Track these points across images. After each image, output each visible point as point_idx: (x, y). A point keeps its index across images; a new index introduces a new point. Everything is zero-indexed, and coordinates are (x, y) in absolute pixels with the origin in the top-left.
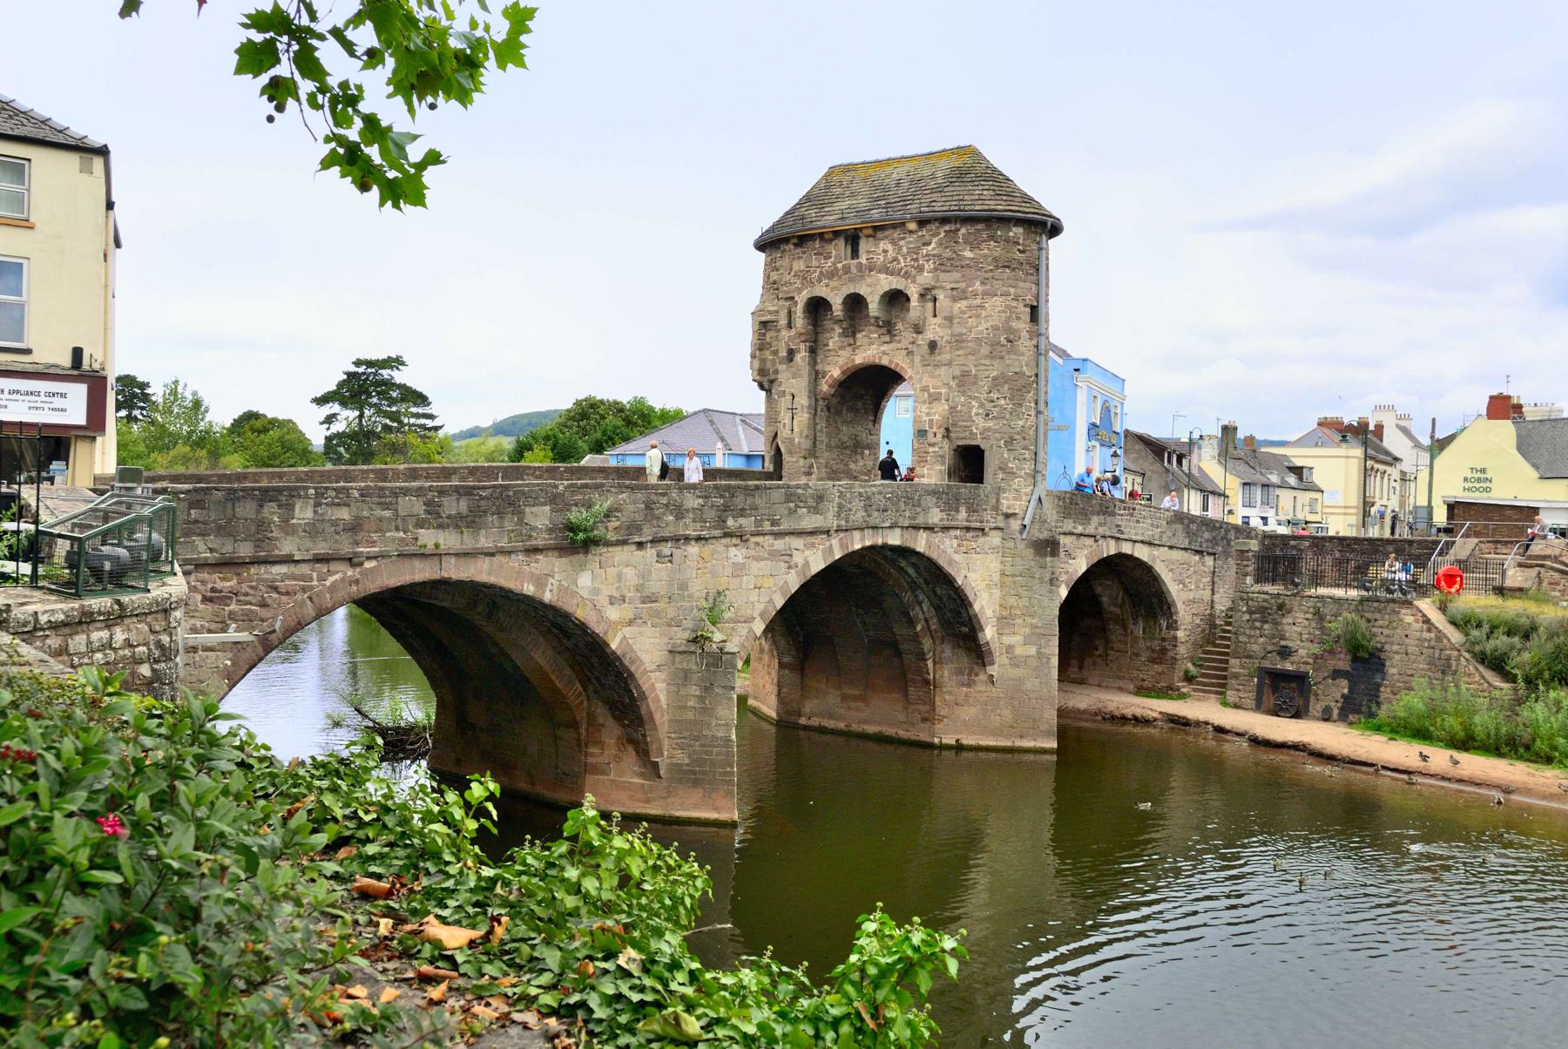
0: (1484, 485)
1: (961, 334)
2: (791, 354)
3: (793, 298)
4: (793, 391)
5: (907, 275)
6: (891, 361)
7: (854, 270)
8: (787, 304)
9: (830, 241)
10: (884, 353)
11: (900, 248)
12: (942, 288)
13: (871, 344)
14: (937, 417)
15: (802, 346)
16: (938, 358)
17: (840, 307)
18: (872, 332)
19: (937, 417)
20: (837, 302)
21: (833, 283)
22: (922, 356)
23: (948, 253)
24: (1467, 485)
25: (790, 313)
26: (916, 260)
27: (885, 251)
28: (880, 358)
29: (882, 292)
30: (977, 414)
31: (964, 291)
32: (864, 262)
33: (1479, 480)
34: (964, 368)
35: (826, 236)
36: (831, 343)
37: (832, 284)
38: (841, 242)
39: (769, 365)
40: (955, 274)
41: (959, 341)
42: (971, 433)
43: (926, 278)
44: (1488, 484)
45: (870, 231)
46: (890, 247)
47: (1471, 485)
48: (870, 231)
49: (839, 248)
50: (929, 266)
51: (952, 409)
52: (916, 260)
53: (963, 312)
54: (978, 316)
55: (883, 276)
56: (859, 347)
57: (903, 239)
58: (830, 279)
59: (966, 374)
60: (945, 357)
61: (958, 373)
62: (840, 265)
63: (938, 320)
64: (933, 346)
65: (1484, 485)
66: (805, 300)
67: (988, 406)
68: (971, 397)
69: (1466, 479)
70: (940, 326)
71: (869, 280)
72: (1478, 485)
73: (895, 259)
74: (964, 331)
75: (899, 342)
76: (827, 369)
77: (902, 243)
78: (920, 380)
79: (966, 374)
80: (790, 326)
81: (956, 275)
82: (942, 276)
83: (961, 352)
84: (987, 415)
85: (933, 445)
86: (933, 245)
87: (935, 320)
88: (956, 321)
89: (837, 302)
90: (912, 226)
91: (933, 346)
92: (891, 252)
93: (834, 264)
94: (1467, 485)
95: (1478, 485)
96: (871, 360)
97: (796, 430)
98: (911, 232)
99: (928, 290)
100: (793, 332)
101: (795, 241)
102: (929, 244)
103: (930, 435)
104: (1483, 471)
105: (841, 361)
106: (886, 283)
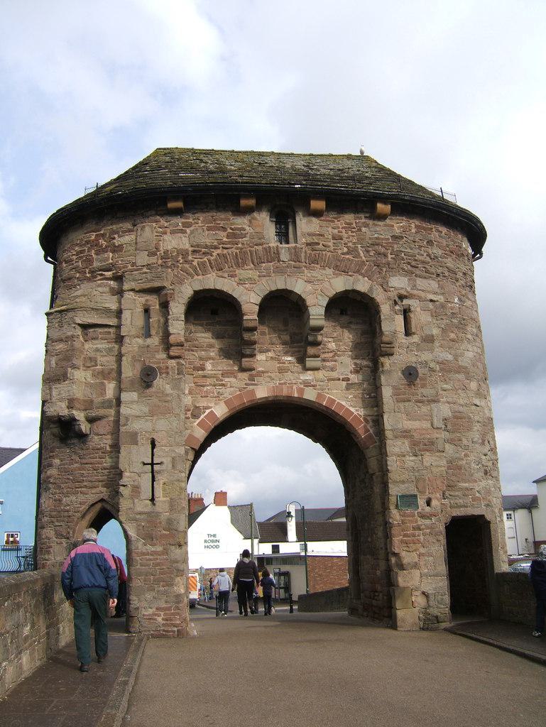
0: (216, 544)
2: (147, 377)
3: (156, 291)
6: (319, 395)
7: (284, 256)
8: (142, 299)
10: (307, 384)
12: (420, 299)
20: (250, 301)
21: (248, 272)
22: (394, 388)
24: (206, 544)
25: (147, 311)
28: (301, 391)
29: (332, 293)
33: (212, 541)
34: (456, 407)
36: (209, 366)
40: (431, 282)
41: (447, 369)
43: (399, 282)
44: (217, 543)
47: (209, 544)
49: (264, 223)
56: (260, 374)
64: (411, 374)
65: (216, 544)
69: (205, 541)
72: (212, 544)
74: (450, 357)
75: (332, 369)
79: (458, 416)
81: (433, 285)
82: (419, 281)
84: (486, 473)
85: (423, 516)
89: (250, 301)
91: (411, 374)
94: (206, 544)
95: (212, 544)
96: (285, 392)
98: (382, 217)
99: (401, 297)
103: (421, 502)
104: (214, 536)
105: (228, 393)
106: (340, 284)
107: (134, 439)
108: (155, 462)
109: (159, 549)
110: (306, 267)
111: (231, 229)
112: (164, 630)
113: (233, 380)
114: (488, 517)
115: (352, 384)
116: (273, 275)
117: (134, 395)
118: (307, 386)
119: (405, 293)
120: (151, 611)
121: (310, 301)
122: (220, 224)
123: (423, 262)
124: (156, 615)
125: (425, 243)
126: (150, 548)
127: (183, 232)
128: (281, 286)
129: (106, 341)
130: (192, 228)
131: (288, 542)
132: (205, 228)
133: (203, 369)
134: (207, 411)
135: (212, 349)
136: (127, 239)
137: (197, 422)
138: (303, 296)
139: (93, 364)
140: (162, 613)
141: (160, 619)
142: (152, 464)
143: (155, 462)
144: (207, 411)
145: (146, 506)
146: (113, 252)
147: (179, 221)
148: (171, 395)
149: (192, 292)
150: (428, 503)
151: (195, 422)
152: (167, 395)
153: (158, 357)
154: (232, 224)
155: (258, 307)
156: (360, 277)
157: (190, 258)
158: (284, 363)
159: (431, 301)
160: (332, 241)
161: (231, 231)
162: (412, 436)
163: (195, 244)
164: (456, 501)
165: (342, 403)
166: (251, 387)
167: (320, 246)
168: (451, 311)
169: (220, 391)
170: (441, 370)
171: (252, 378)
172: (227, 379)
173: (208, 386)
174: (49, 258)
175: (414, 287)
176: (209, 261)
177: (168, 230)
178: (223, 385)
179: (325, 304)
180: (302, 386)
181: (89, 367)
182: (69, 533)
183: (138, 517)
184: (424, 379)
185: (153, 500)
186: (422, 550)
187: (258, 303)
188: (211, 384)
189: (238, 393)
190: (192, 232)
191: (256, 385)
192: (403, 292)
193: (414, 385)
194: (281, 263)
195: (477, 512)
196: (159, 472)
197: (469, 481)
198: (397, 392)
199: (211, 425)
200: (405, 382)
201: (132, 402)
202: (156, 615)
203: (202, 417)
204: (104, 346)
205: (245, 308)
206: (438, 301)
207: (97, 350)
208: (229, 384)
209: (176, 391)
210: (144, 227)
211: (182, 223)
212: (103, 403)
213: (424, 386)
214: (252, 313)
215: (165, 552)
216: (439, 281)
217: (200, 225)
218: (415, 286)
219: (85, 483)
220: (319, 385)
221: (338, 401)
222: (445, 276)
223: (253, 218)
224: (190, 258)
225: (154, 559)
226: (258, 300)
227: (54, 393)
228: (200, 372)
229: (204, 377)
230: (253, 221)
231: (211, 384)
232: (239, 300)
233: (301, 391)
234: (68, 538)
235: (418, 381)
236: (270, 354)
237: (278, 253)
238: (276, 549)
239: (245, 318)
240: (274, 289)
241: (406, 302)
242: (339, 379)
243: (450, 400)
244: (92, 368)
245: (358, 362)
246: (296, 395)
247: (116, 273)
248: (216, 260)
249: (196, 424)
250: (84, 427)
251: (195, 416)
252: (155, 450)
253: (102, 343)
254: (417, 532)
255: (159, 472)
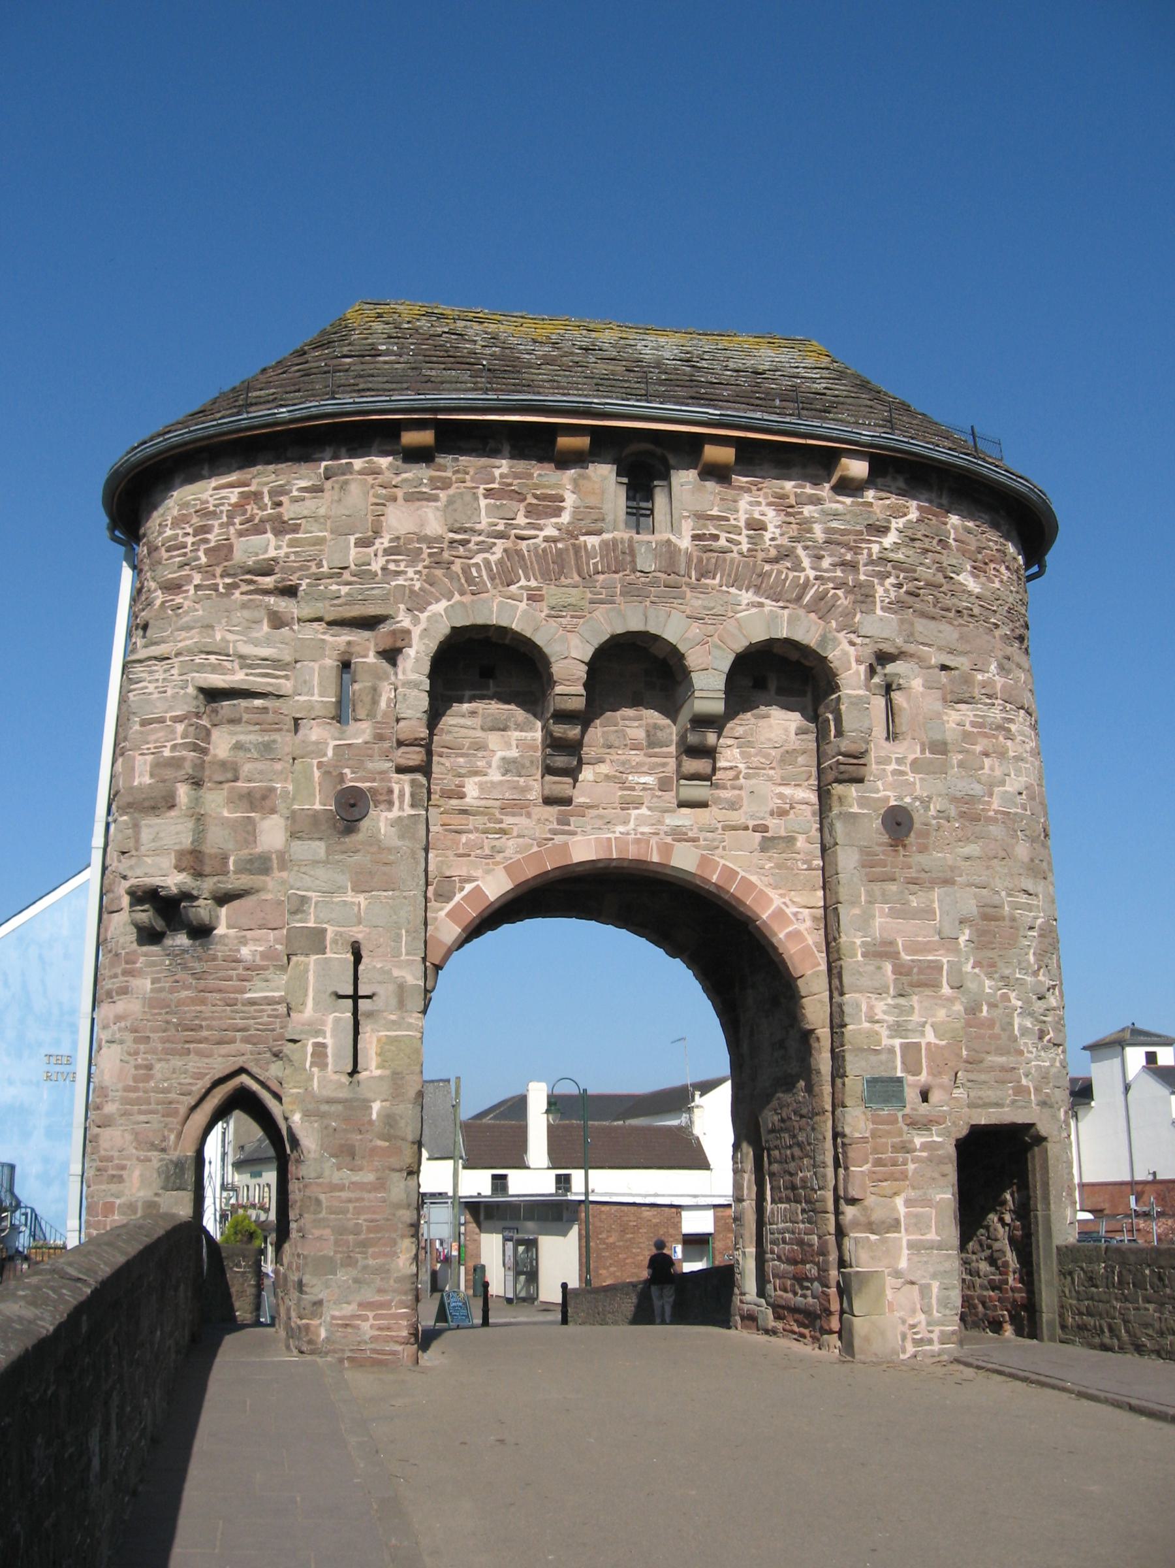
1: (970, 799)
3: (369, 623)
4: (358, 933)
5: (822, 607)
6: (704, 861)
7: (646, 562)
9: (565, 461)
10: (679, 835)
11: (805, 525)
13: (627, 804)
14: (930, 1037)
15: (402, 785)
16: (918, 859)
17: (581, 672)
18: (637, 770)
19: (930, 1037)
21: (569, 592)
22: (865, 851)
23: (926, 572)
26: (853, 566)
27: (756, 526)
28: (666, 849)
29: (740, 645)
30: (1024, 1031)
31: (967, 680)
32: (685, 543)
35: (564, 442)
36: (471, 789)
37: (553, 593)
38: (604, 474)
39: (217, 839)
40: (944, 626)
42: (1020, 1090)
45: (724, 455)
46: (771, 517)
48: (724, 455)
50: (884, 591)
51: (972, 1010)
52: (853, 566)
53: (966, 736)
54: (1002, 755)
55: (747, 596)
57: (816, 501)
58: (546, 576)
59: (989, 915)
60: (938, 858)
61: (969, 904)
62: (592, 541)
63: (909, 749)
66: (443, 630)
67: (1039, 1006)
68: (1007, 981)
70: (916, 765)
71: (695, 602)
73: (785, 554)
74: (978, 789)
75: (733, 806)
76: (458, 869)
77: (808, 510)
78: (867, 918)
79: (989, 915)
80: (341, 714)
81: (947, 632)
82: (921, 625)
83: (972, 849)
85: (915, 1124)
86: (890, 539)
87: (898, 749)
88: (956, 758)
90: (858, 468)
92: (772, 531)
93: (570, 533)
96: (632, 853)
97: (372, 1068)
98: (846, 487)
99: (883, 658)
100: (360, 733)
101: (426, 437)
102: (883, 530)
103: (911, 1095)
107: (315, 941)
108: (361, 993)
109: (369, 1177)
110: (688, 585)
111: (535, 496)
112: (374, 1351)
113: (522, 821)
114: (1043, 1129)
115: (773, 838)
116: (618, 599)
117: (318, 848)
118: (679, 841)
119: (892, 650)
120: (349, 1309)
121: (693, 659)
122: (511, 485)
123: (929, 584)
124: (359, 1317)
125: (935, 542)
126: (345, 1176)
127: (435, 499)
128: (635, 624)
129: (258, 727)
130: (451, 491)
131: (528, 1168)
132: (481, 491)
133: (462, 796)
134: (468, 887)
135: (480, 754)
136: (310, 505)
137: (442, 914)
138: (682, 648)
139: (230, 776)
140: (371, 1314)
141: (366, 1326)
142: (355, 997)
143: (361, 993)
144: (468, 887)
145: (341, 1085)
146: (278, 533)
147: (420, 473)
148: (397, 850)
149: (447, 631)
150: (925, 1097)
151: (441, 909)
152: (389, 850)
153: (370, 765)
154: (537, 486)
155: (586, 668)
156: (802, 612)
157: (446, 555)
158: (633, 789)
159: (944, 668)
160: (745, 532)
161: (535, 501)
162: (894, 956)
163: (457, 525)
164: (981, 1093)
165: (754, 879)
166: (559, 839)
167: (722, 542)
168: (983, 691)
169: (496, 843)
170: (962, 815)
171: (563, 821)
172: (509, 820)
173: (470, 832)
174: (117, 533)
175: (910, 637)
176: (487, 562)
177: (400, 493)
178: (503, 832)
179: (726, 665)
180: (669, 840)
181: (221, 783)
182: (164, 1139)
183: (325, 1108)
184: (925, 834)
185: (354, 1072)
186: (912, 1194)
187: (587, 659)
188: (477, 830)
189: (535, 849)
190: (451, 501)
191: (574, 833)
192: (887, 648)
193: (904, 846)
194: (639, 574)
195: (1020, 1118)
196: (370, 1015)
197: (1008, 1053)
198: (868, 862)
199: (473, 913)
200: (885, 838)
201: (316, 863)
202: (359, 1317)
203: (458, 897)
204: (252, 737)
205: (557, 669)
206: (956, 669)
207: (238, 746)
208: (515, 828)
209: (407, 843)
210: (346, 482)
211: (431, 479)
212: (251, 861)
213: (923, 849)
214: (571, 681)
215: (381, 1185)
216: (960, 625)
217: (469, 484)
218: (912, 634)
219: (205, 1033)
220: (705, 840)
221: (742, 873)
222: (972, 616)
223: (581, 476)
224: (446, 555)
225: (358, 1200)
226: (587, 653)
227: (146, 835)
228: (454, 802)
229: (464, 812)
230: (581, 482)
231: (477, 830)
232: (546, 650)
233: (666, 849)
234: (163, 1150)
235: (912, 839)
236: (604, 769)
237: (632, 553)
238: (500, 1182)
239: (558, 689)
240: (620, 630)
241: (890, 668)
242: (746, 828)
243: (977, 880)
244: (226, 786)
245: (787, 791)
246: (655, 859)
247: (283, 580)
248: (500, 562)
249: (442, 914)
250: (202, 910)
251: (444, 896)
252: (361, 967)
253: (251, 732)
254: (900, 1157)
255: (370, 1015)
